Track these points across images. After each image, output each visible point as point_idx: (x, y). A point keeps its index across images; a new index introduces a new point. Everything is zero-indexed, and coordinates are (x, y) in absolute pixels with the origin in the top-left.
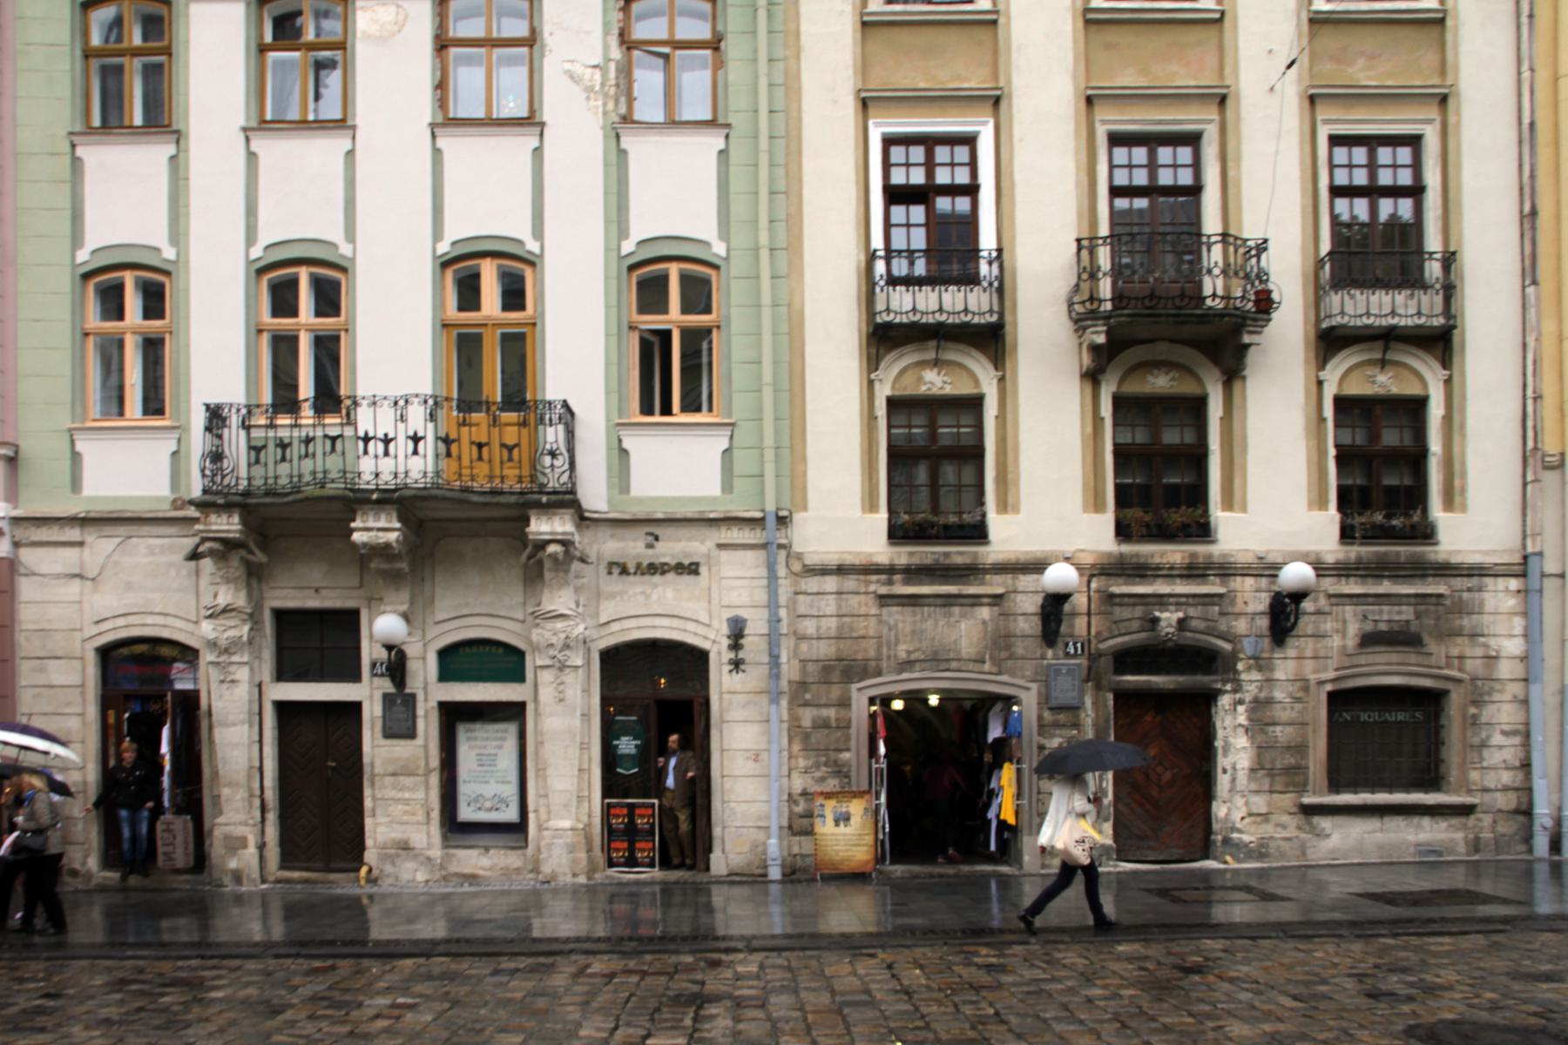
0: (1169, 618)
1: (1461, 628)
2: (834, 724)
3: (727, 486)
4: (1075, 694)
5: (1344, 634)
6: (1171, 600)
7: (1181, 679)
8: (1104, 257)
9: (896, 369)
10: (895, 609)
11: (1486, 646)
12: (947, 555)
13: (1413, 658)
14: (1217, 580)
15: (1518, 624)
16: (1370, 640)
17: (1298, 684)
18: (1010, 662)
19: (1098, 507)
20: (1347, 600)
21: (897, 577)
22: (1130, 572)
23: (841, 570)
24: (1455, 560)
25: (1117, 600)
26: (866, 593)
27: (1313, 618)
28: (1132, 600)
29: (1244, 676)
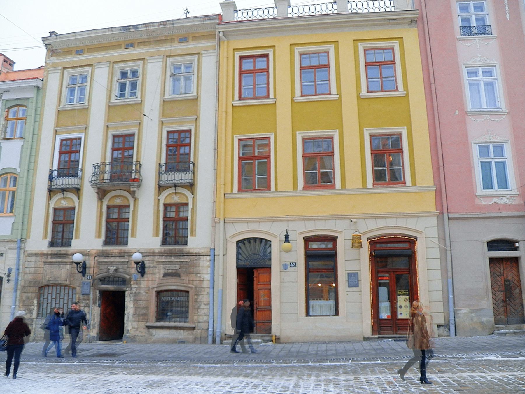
0: (112, 268)
1: (193, 271)
2: (30, 298)
3: (12, 233)
4: (88, 290)
5: (159, 273)
6: (115, 263)
7: (115, 286)
8: (108, 168)
9: (108, 199)
10: (47, 266)
11: (200, 277)
12: (60, 250)
13: (179, 281)
14: (127, 257)
15: (209, 270)
16: (166, 275)
17: (147, 288)
18: (74, 281)
19: (99, 236)
20: (161, 263)
21: (49, 257)
22: (105, 255)
23: (36, 255)
24: (191, 251)
25: (101, 263)
26: (41, 261)
27: (152, 268)
28: (104, 263)
29: (132, 286)
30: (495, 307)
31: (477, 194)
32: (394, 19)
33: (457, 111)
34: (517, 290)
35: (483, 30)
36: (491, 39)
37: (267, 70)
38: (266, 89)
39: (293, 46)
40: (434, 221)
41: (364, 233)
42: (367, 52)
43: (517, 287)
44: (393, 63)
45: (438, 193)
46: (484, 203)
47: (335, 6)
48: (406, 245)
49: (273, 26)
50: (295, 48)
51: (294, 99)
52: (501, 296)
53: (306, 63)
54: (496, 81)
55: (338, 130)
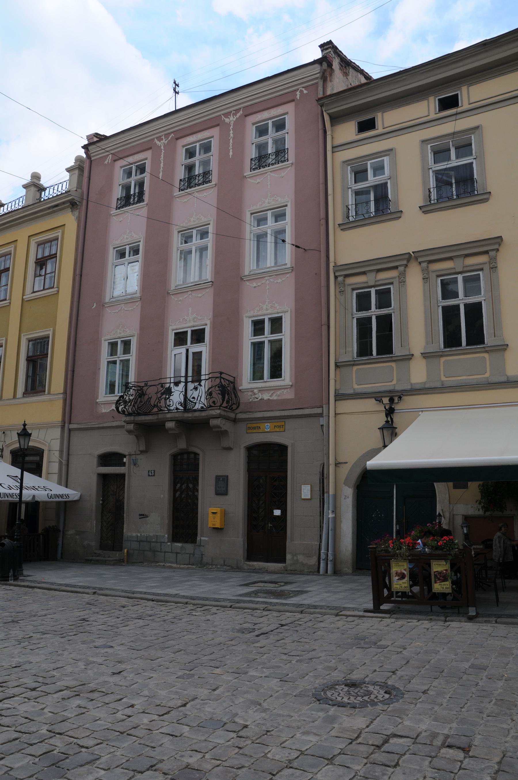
31: (97, 401)
33: (95, 303)
41: (8, 446)
45: (65, 400)
46: (104, 411)
48: (37, 458)
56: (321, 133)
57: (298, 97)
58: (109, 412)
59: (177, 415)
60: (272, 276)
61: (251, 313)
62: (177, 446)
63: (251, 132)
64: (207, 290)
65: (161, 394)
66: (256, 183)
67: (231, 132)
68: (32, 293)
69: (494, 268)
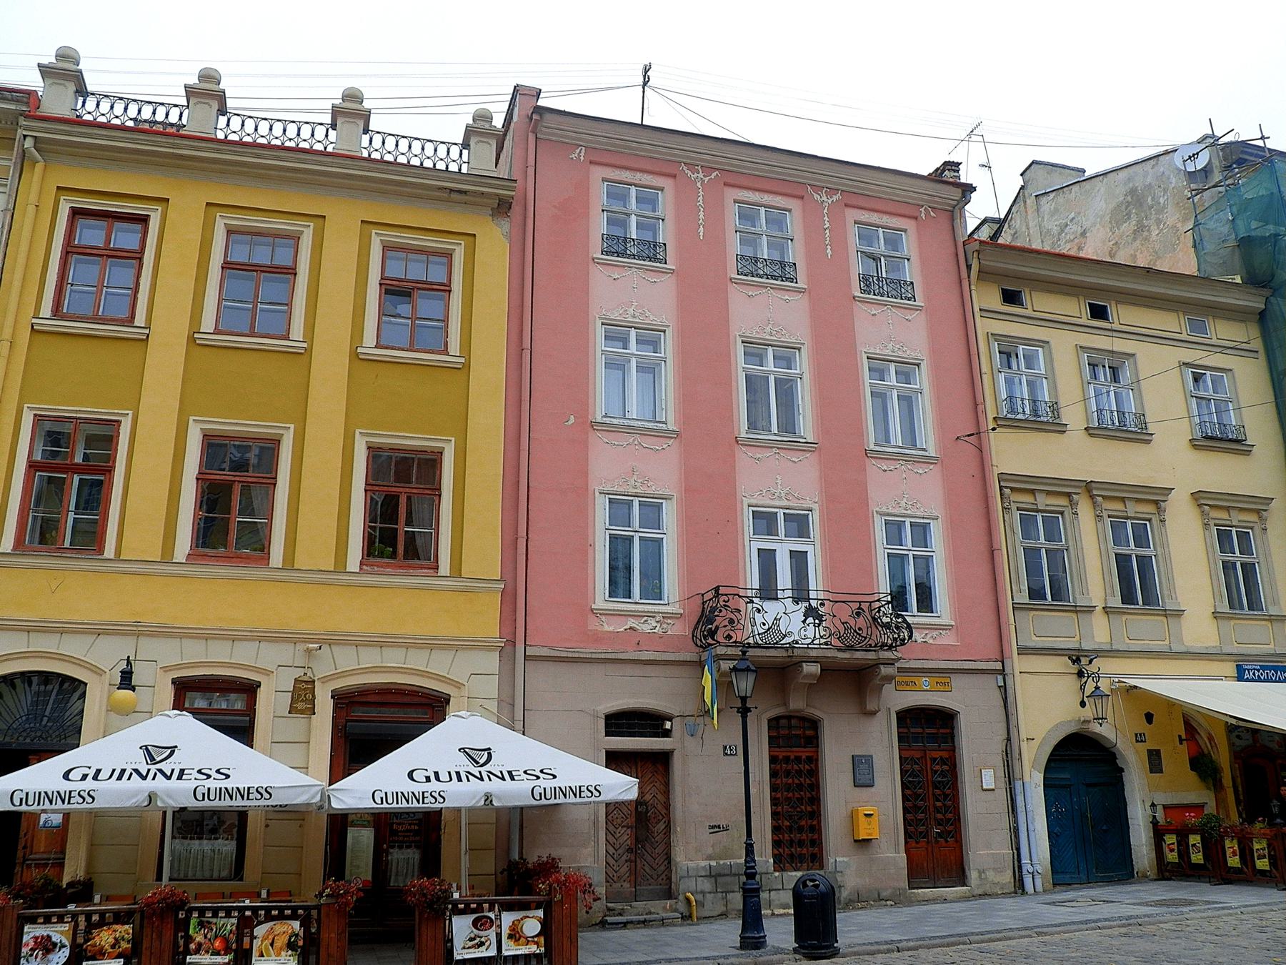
30: (612, 862)
32: (460, 192)
34: (661, 826)
35: (651, 252)
36: (663, 272)
37: (138, 256)
38: (128, 301)
39: (213, 209)
40: (491, 662)
41: (325, 680)
42: (389, 254)
43: (661, 817)
44: (446, 289)
45: (509, 598)
46: (607, 628)
47: (332, 134)
49: (171, 150)
50: (218, 214)
51: (196, 336)
52: (625, 837)
53: (240, 255)
54: (663, 362)
55: (292, 426)
56: (965, 283)
57: (923, 215)
58: (622, 632)
59: (829, 654)
60: (909, 461)
61: (884, 510)
62: (785, 704)
63: (853, 233)
64: (808, 455)
65: (804, 616)
66: (872, 313)
67: (826, 218)
68: (376, 347)
69: (1163, 521)
